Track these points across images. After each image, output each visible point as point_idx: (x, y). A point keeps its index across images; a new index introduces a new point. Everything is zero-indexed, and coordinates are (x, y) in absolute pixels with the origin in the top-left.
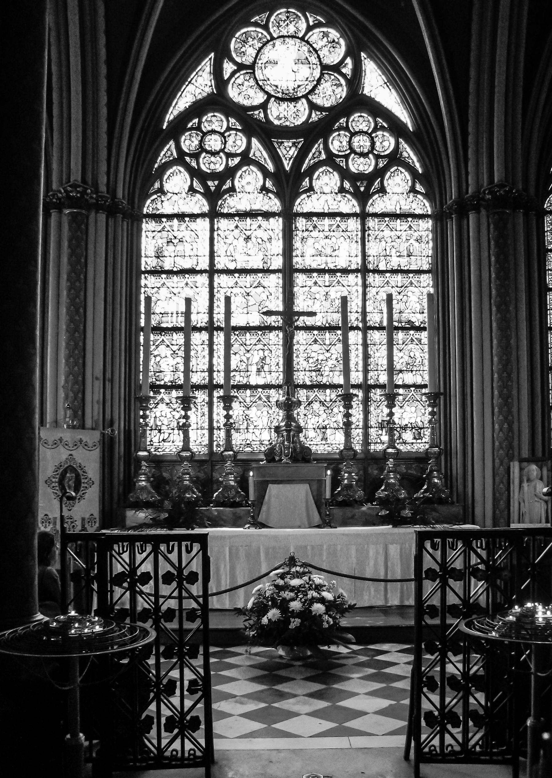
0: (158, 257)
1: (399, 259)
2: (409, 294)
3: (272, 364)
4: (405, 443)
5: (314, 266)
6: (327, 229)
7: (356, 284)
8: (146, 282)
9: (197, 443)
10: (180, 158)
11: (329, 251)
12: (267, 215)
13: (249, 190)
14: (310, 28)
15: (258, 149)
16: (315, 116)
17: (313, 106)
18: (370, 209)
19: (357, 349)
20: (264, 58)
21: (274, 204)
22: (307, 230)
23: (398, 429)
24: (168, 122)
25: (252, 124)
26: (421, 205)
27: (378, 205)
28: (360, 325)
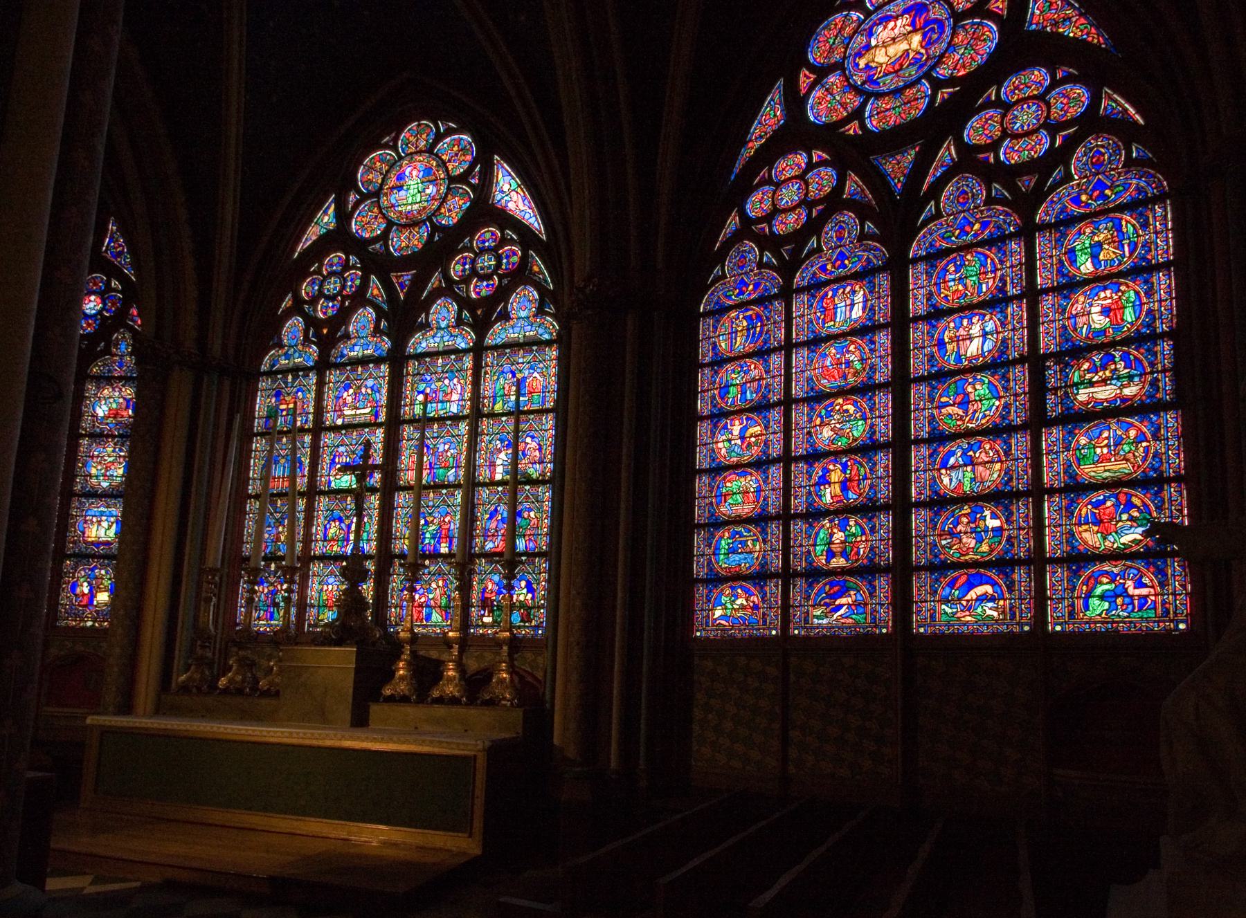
6: (440, 370)
10: (298, 307)
13: (363, 335)
15: (375, 289)
17: (436, 228)
18: (488, 342)
20: (392, 181)
22: (418, 374)
27: (499, 334)
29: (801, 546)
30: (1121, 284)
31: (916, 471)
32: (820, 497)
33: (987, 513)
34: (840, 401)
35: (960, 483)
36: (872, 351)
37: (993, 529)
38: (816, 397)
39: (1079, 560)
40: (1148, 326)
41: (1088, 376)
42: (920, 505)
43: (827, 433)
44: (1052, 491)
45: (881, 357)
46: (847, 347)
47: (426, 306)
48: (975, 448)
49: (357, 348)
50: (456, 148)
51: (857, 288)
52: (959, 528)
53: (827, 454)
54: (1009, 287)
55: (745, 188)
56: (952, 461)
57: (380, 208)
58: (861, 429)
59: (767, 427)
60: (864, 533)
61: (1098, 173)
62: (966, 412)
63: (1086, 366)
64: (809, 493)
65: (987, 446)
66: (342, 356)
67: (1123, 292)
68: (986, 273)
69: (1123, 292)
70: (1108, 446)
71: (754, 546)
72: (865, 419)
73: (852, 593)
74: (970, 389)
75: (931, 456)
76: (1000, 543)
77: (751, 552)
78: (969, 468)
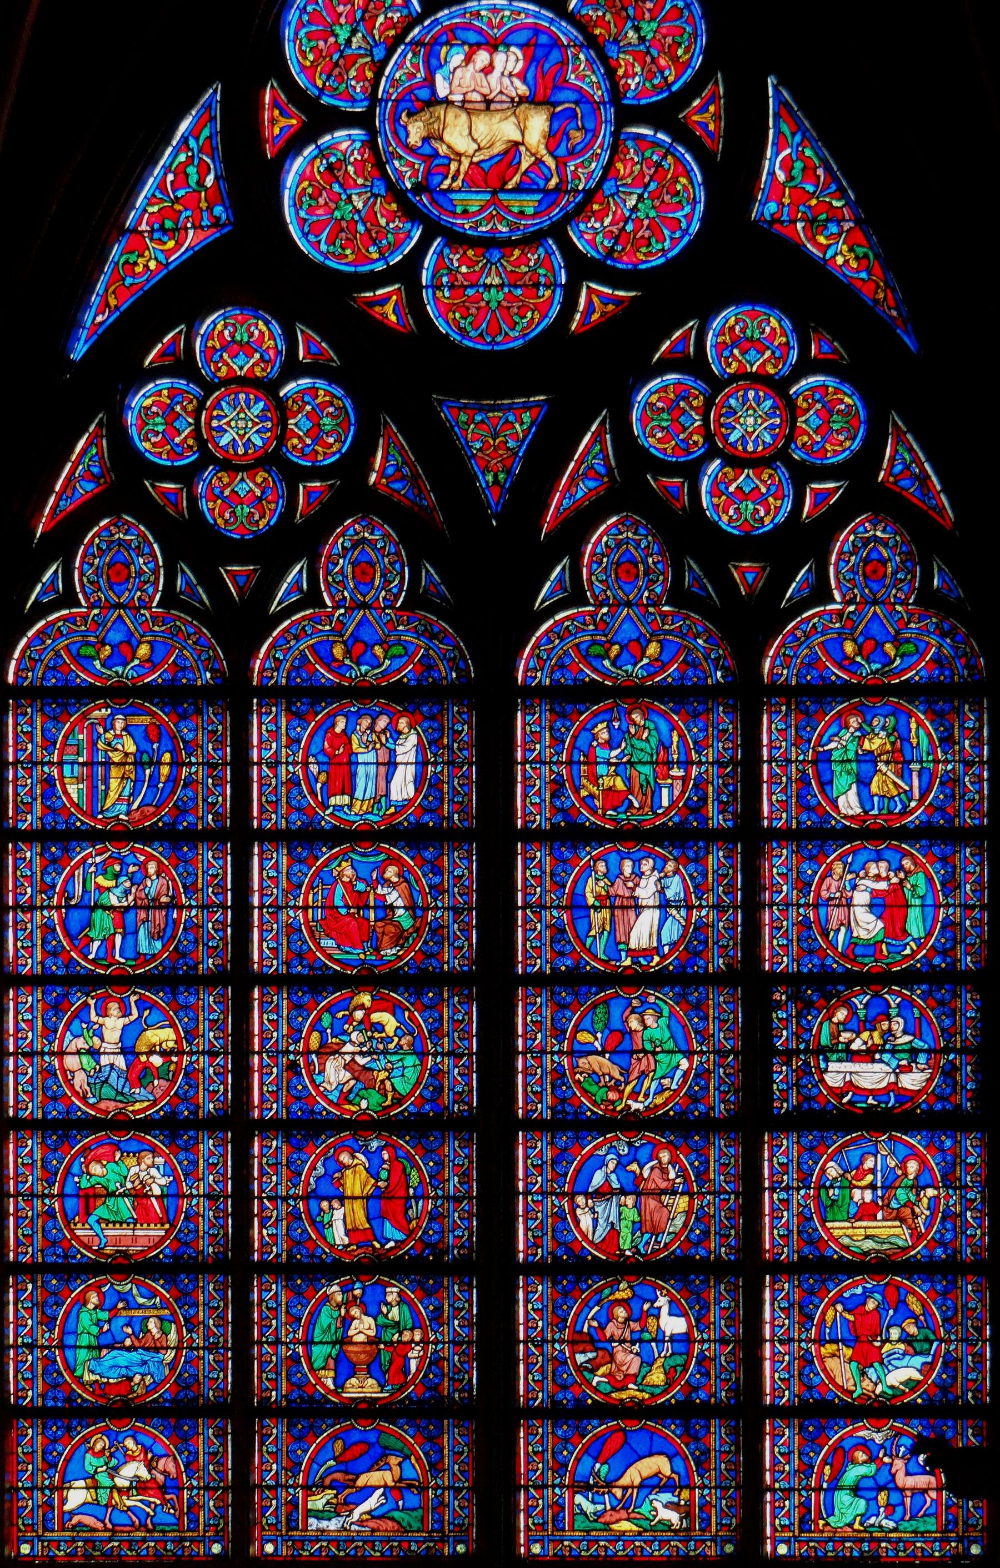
29: (277, 1342)
30: (906, 854)
31: (527, 1193)
32: (320, 1227)
33: (662, 1302)
34: (366, 999)
35: (614, 1233)
36: (437, 890)
37: (673, 1339)
38: (311, 982)
39: (821, 1411)
40: (944, 953)
41: (845, 1036)
42: (535, 1269)
43: (335, 1074)
44: (778, 1268)
45: (456, 911)
46: (382, 868)
48: (643, 1154)
51: (403, 723)
52: (611, 1329)
53: (336, 1125)
54: (712, 809)
55: (119, 363)
56: (598, 1179)
58: (412, 1075)
59: (191, 1034)
60: (417, 1323)
61: (875, 602)
62: (626, 1071)
63: (841, 1015)
64: (294, 1216)
65: (665, 1156)
67: (908, 873)
68: (669, 764)
69: (908, 873)
70: (873, 1186)
71: (165, 1334)
72: (422, 1055)
73: (393, 1460)
74: (634, 1024)
75: (555, 1162)
76: (685, 1369)
77: (157, 1349)
78: (630, 1200)
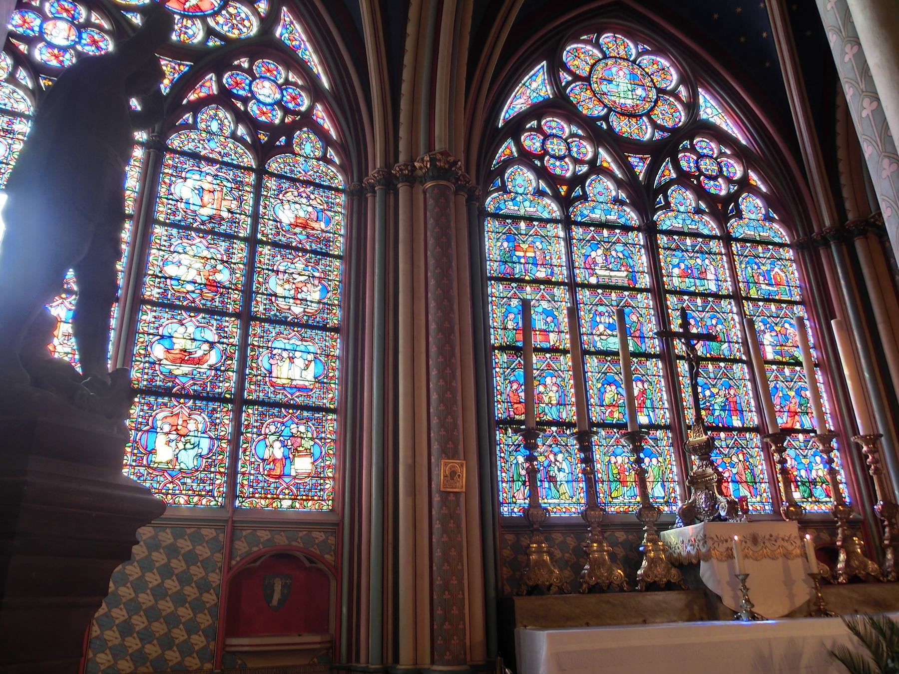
0: (506, 262)
1: (768, 288)
2: (787, 326)
3: (654, 399)
4: (818, 502)
5: (683, 287)
7: (731, 311)
8: (494, 290)
9: (574, 500)
11: (696, 274)
12: (626, 229)
14: (639, 54)
15: (606, 158)
16: (658, 135)
19: (745, 386)
21: (632, 217)
23: (807, 484)
24: (504, 119)
25: (597, 132)
26: (779, 232)
28: (744, 358)
47: (664, 189)
49: (597, 211)
50: (655, 66)
57: (593, 92)
66: (582, 215)
